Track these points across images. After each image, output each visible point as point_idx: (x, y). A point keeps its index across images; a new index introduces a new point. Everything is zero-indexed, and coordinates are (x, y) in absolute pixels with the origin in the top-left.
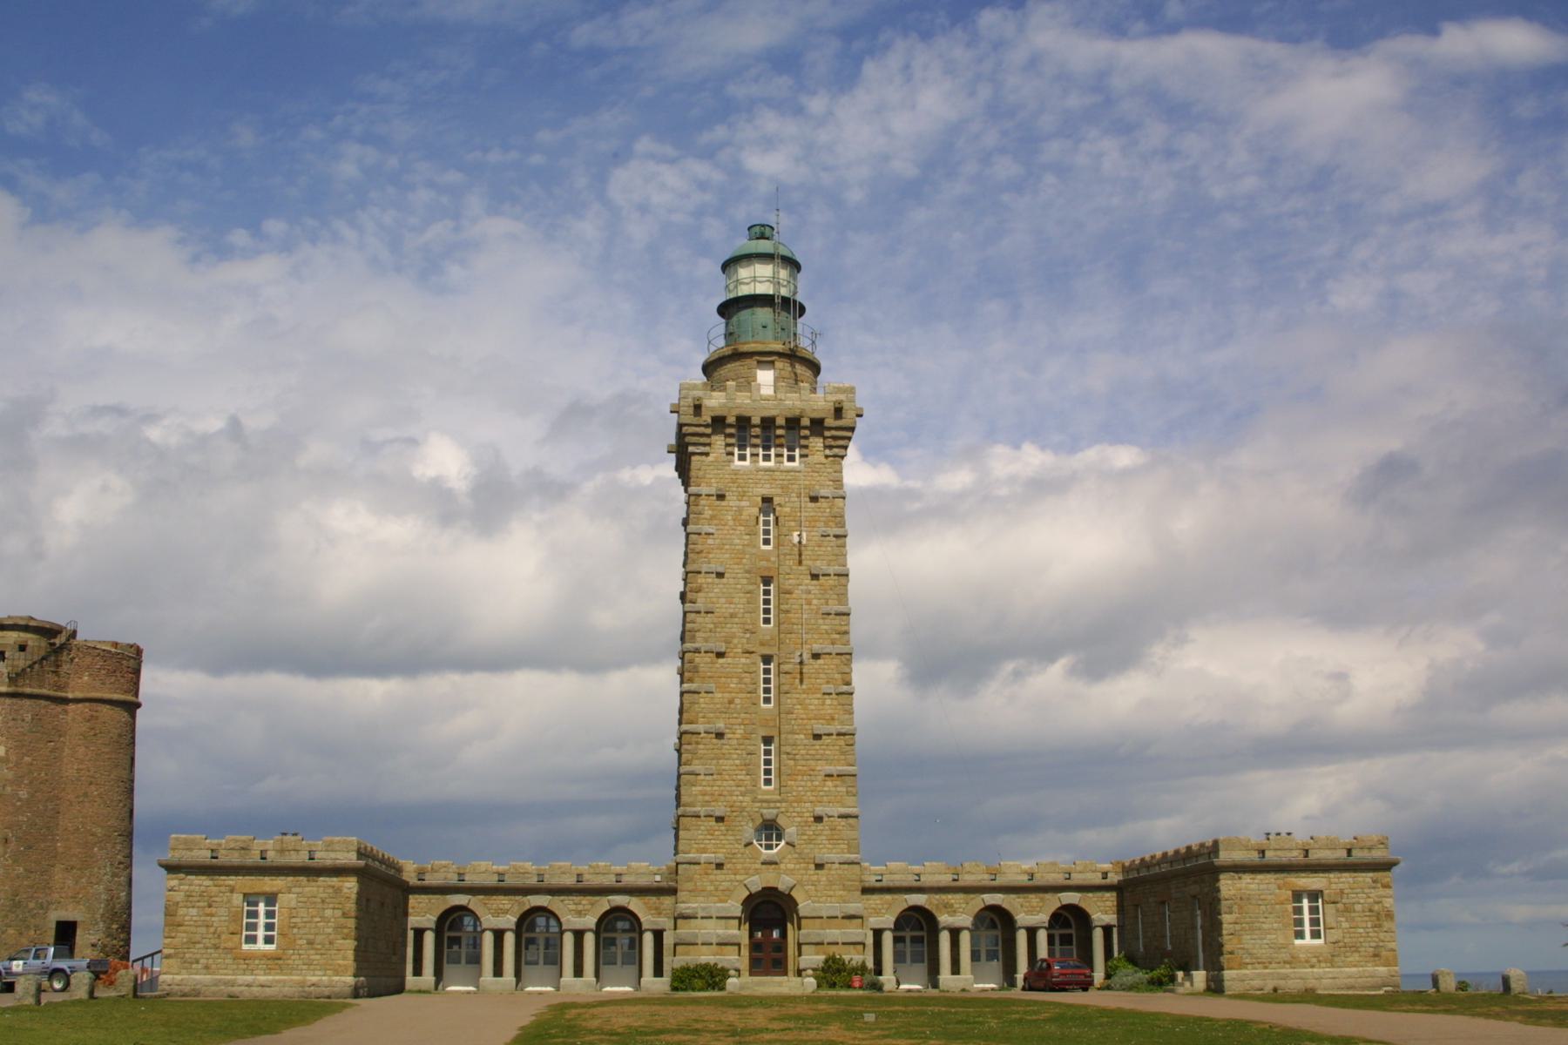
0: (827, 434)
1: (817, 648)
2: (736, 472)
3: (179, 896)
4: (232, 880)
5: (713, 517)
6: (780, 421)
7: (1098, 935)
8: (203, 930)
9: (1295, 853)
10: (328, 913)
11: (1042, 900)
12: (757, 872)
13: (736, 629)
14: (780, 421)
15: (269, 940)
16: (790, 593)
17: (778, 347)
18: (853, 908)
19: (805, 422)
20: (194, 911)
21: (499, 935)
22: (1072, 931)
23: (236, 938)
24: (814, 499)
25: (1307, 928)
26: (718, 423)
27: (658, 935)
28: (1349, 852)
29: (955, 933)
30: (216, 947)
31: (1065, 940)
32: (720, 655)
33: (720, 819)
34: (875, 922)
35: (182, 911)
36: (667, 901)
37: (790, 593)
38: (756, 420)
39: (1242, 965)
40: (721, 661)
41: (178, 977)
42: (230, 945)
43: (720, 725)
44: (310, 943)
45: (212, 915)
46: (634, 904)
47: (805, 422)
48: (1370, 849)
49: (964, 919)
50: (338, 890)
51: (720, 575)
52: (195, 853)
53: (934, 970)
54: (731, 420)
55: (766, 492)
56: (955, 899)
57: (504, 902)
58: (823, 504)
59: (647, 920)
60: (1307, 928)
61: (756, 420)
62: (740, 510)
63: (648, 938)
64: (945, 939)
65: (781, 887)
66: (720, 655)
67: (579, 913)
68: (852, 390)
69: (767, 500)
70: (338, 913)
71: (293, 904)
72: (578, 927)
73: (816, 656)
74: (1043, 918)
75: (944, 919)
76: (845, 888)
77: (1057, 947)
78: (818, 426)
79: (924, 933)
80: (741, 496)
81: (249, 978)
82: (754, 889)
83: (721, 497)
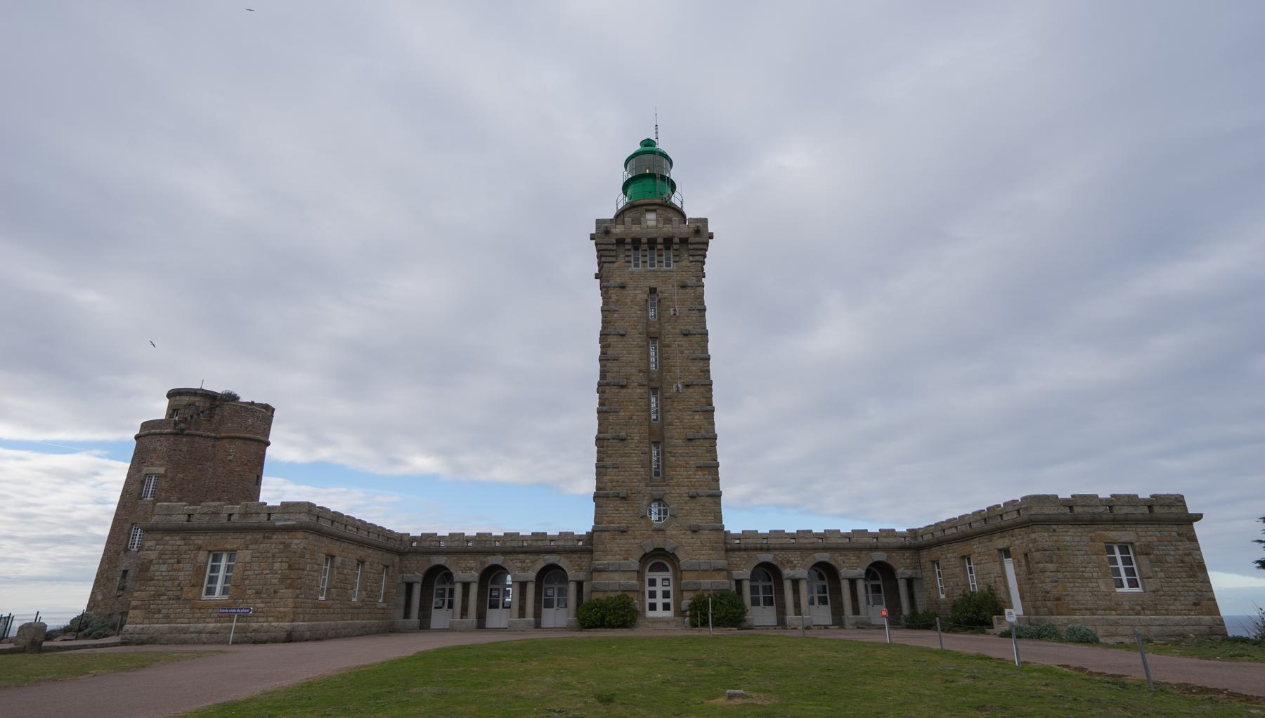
0: (691, 247)
1: (687, 381)
2: (632, 273)
3: (153, 555)
4: (199, 540)
5: (617, 301)
6: (660, 240)
7: (845, 586)
8: (169, 583)
9: (1101, 509)
10: (277, 565)
11: (859, 558)
12: (650, 537)
13: (634, 371)
14: (660, 240)
15: (225, 591)
16: (668, 346)
17: (659, 201)
18: (722, 563)
19: (676, 240)
20: (164, 568)
21: (466, 586)
22: (880, 582)
23: (196, 590)
24: (684, 287)
25: (1124, 577)
26: (620, 242)
27: (580, 585)
28: (1150, 507)
29: (796, 583)
30: (178, 598)
31: (876, 589)
32: (623, 387)
33: (624, 498)
34: (737, 574)
35: (152, 568)
36: (585, 560)
37: (668, 346)
38: (644, 240)
39: (1071, 611)
40: (624, 391)
41: (140, 626)
42: (190, 595)
43: (623, 434)
44: (258, 593)
45: (179, 570)
46: (562, 562)
47: (676, 240)
48: (1169, 506)
49: (801, 572)
50: (287, 546)
51: (623, 335)
52: (174, 518)
53: (781, 611)
54: (628, 240)
55: (653, 284)
56: (795, 557)
57: (472, 562)
58: (689, 290)
59: (572, 574)
60: (1124, 577)
61: (644, 240)
62: (636, 296)
63: (572, 588)
64: (788, 586)
65: (668, 548)
66: (623, 387)
67: (523, 570)
68: (705, 221)
69: (653, 291)
70: (285, 566)
71: (248, 559)
72: (522, 579)
73: (687, 386)
74: (861, 571)
75: (787, 572)
76: (713, 548)
77: (870, 595)
78: (684, 241)
79: (772, 583)
80: (636, 288)
81: (200, 626)
82: (648, 550)
83: (623, 287)
